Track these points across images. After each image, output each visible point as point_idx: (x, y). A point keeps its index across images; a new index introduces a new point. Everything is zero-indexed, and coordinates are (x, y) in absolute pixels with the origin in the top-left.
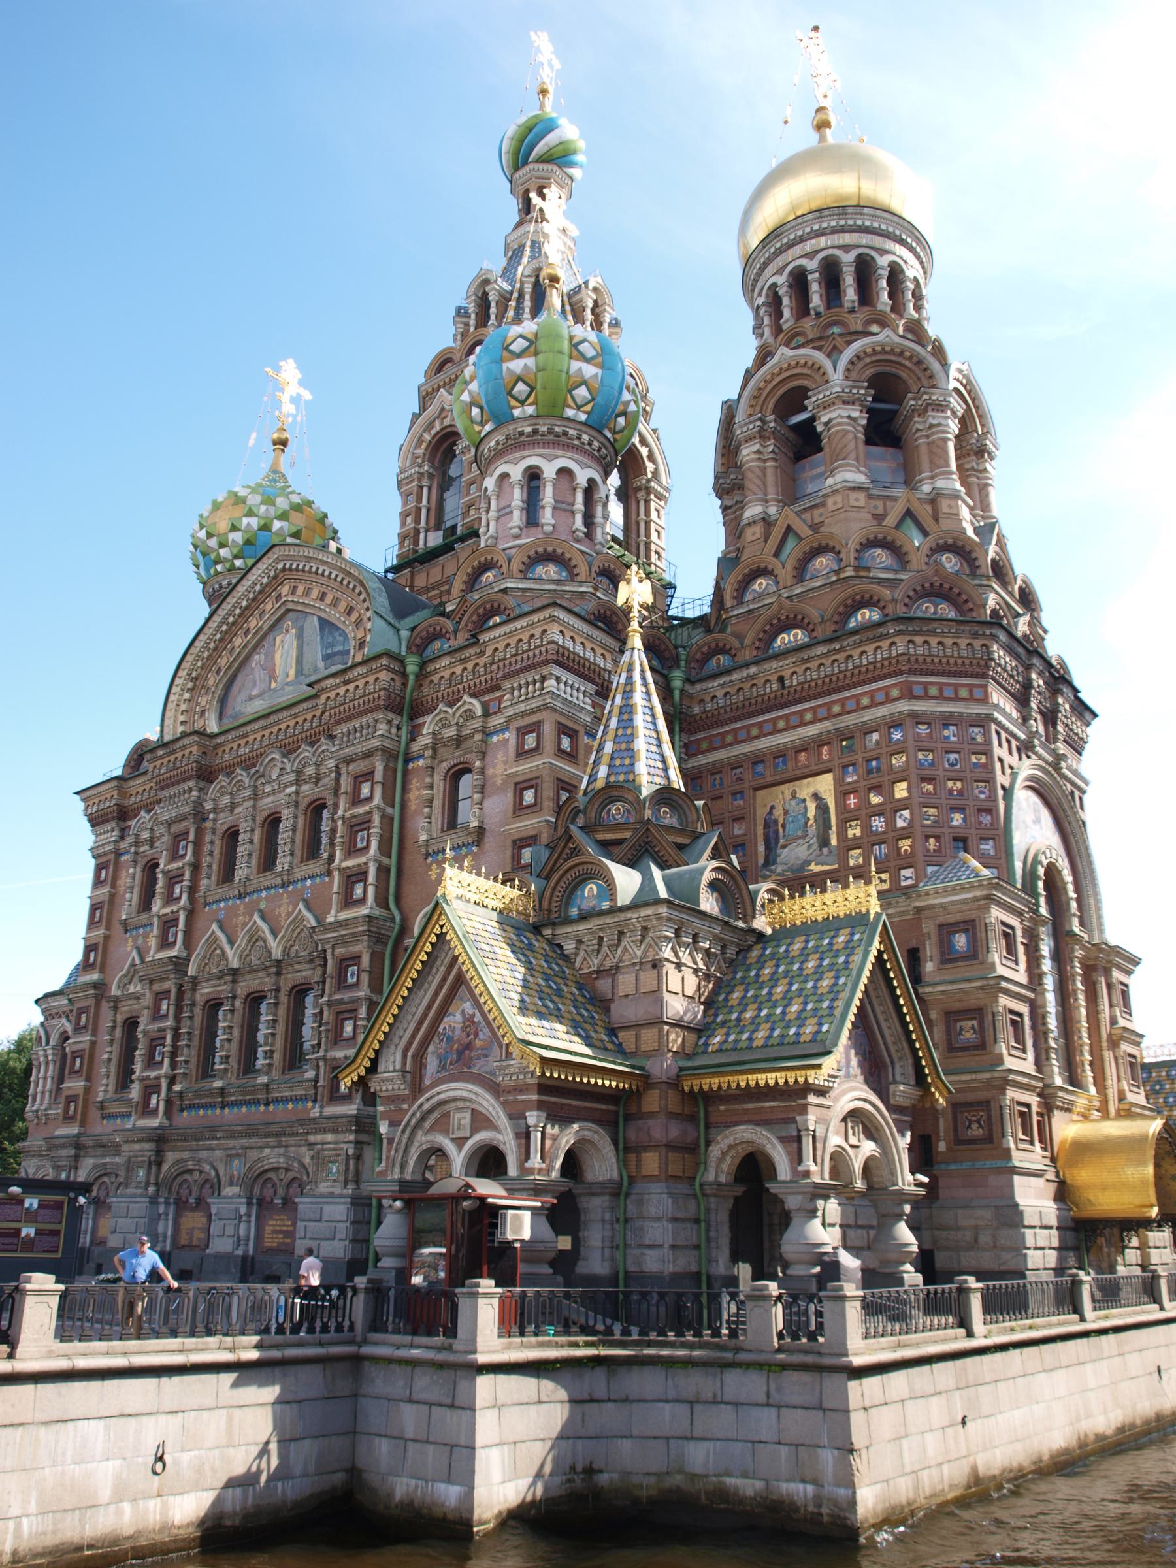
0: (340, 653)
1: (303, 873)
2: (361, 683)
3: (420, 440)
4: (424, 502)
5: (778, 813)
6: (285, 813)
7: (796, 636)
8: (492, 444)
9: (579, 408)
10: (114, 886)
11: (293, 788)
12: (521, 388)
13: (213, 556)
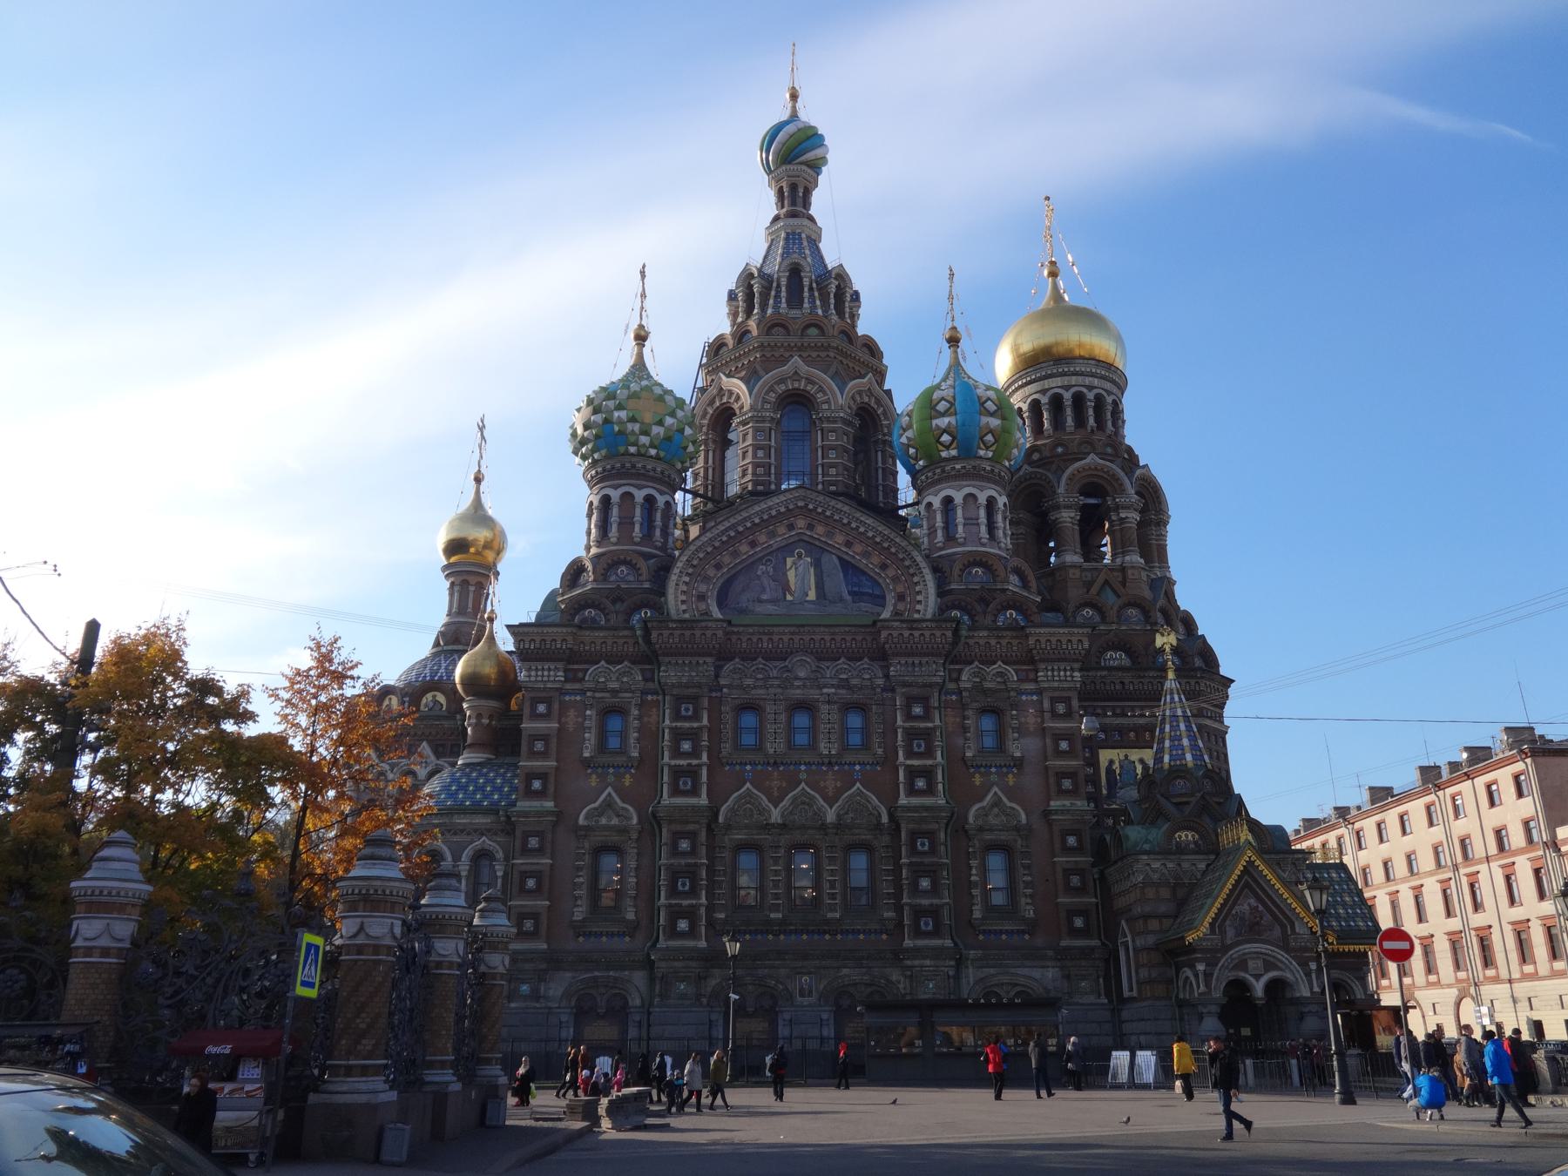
0: (867, 594)
1: (852, 760)
2: (927, 633)
3: (771, 389)
4: (773, 443)
5: (1116, 766)
6: (824, 708)
7: (1121, 655)
8: (958, 467)
9: (1009, 460)
10: (559, 722)
11: (833, 690)
12: (989, 438)
13: (632, 439)
